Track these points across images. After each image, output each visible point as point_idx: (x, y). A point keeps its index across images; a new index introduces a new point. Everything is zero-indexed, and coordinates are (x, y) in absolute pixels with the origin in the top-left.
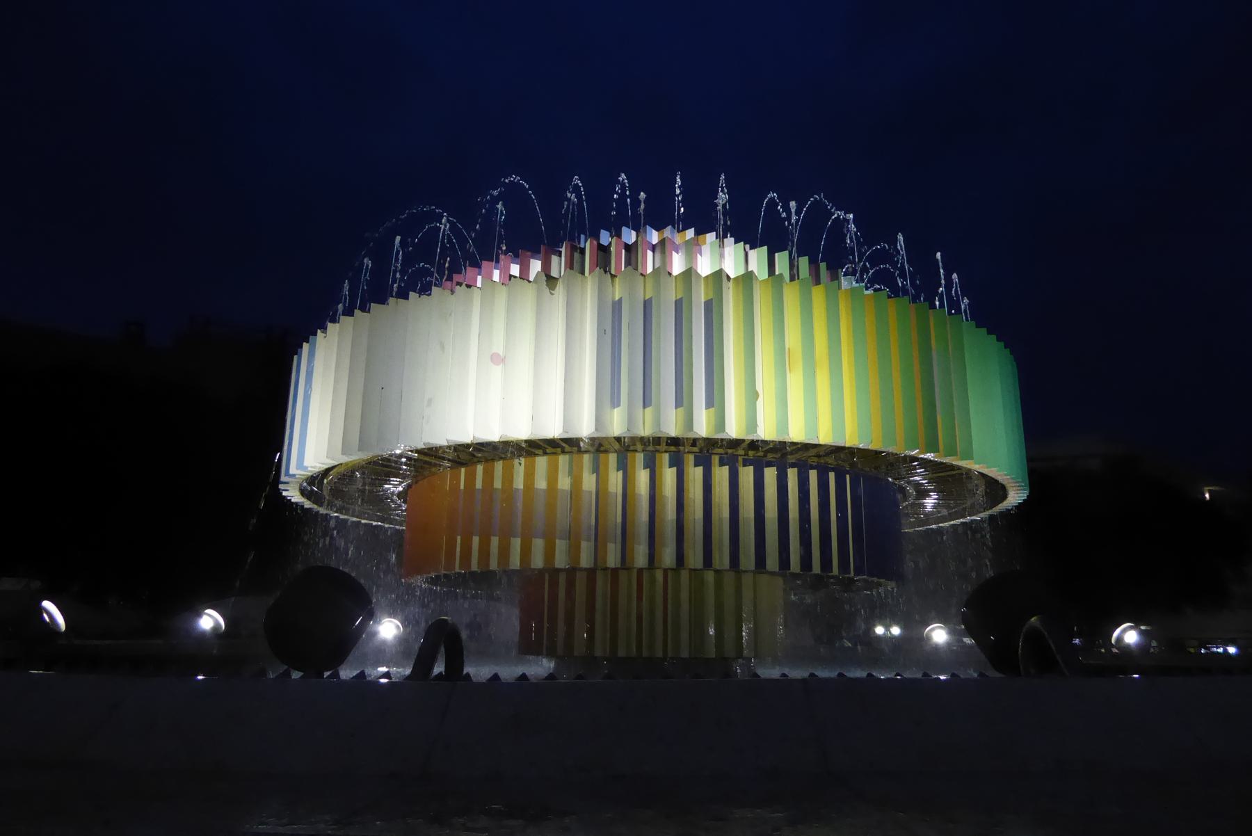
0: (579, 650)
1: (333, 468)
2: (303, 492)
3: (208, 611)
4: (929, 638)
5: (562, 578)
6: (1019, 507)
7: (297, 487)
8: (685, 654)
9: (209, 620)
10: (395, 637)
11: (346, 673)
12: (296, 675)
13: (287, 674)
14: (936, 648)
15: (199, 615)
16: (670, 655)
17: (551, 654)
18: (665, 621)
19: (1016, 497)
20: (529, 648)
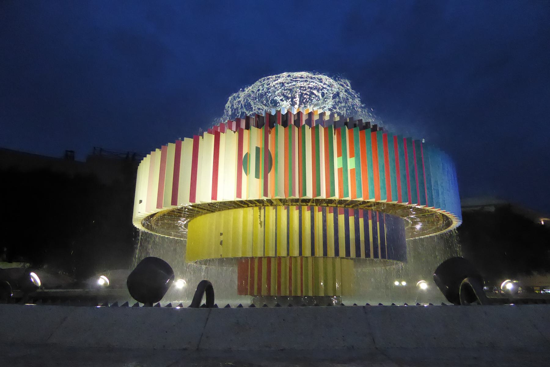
0: (264, 292)
1: (156, 214)
2: (143, 225)
3: (102, 277)
4: (418, 287)
5: (256, 261)
6: (459, 229)
7: (140, 222)
8: (310, 294)
9: (102, 281)
10: (183, 288)
11: (163, 303)
12: (141, 305)
13: (137, 305)
14: (422, 291)
15: (98, 278)
16: (304, 294)
17: (252, 294)
18: (302, 280)
19: (456, 223)
20: (242, 291)
